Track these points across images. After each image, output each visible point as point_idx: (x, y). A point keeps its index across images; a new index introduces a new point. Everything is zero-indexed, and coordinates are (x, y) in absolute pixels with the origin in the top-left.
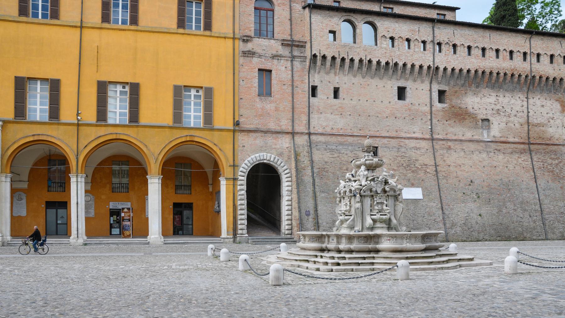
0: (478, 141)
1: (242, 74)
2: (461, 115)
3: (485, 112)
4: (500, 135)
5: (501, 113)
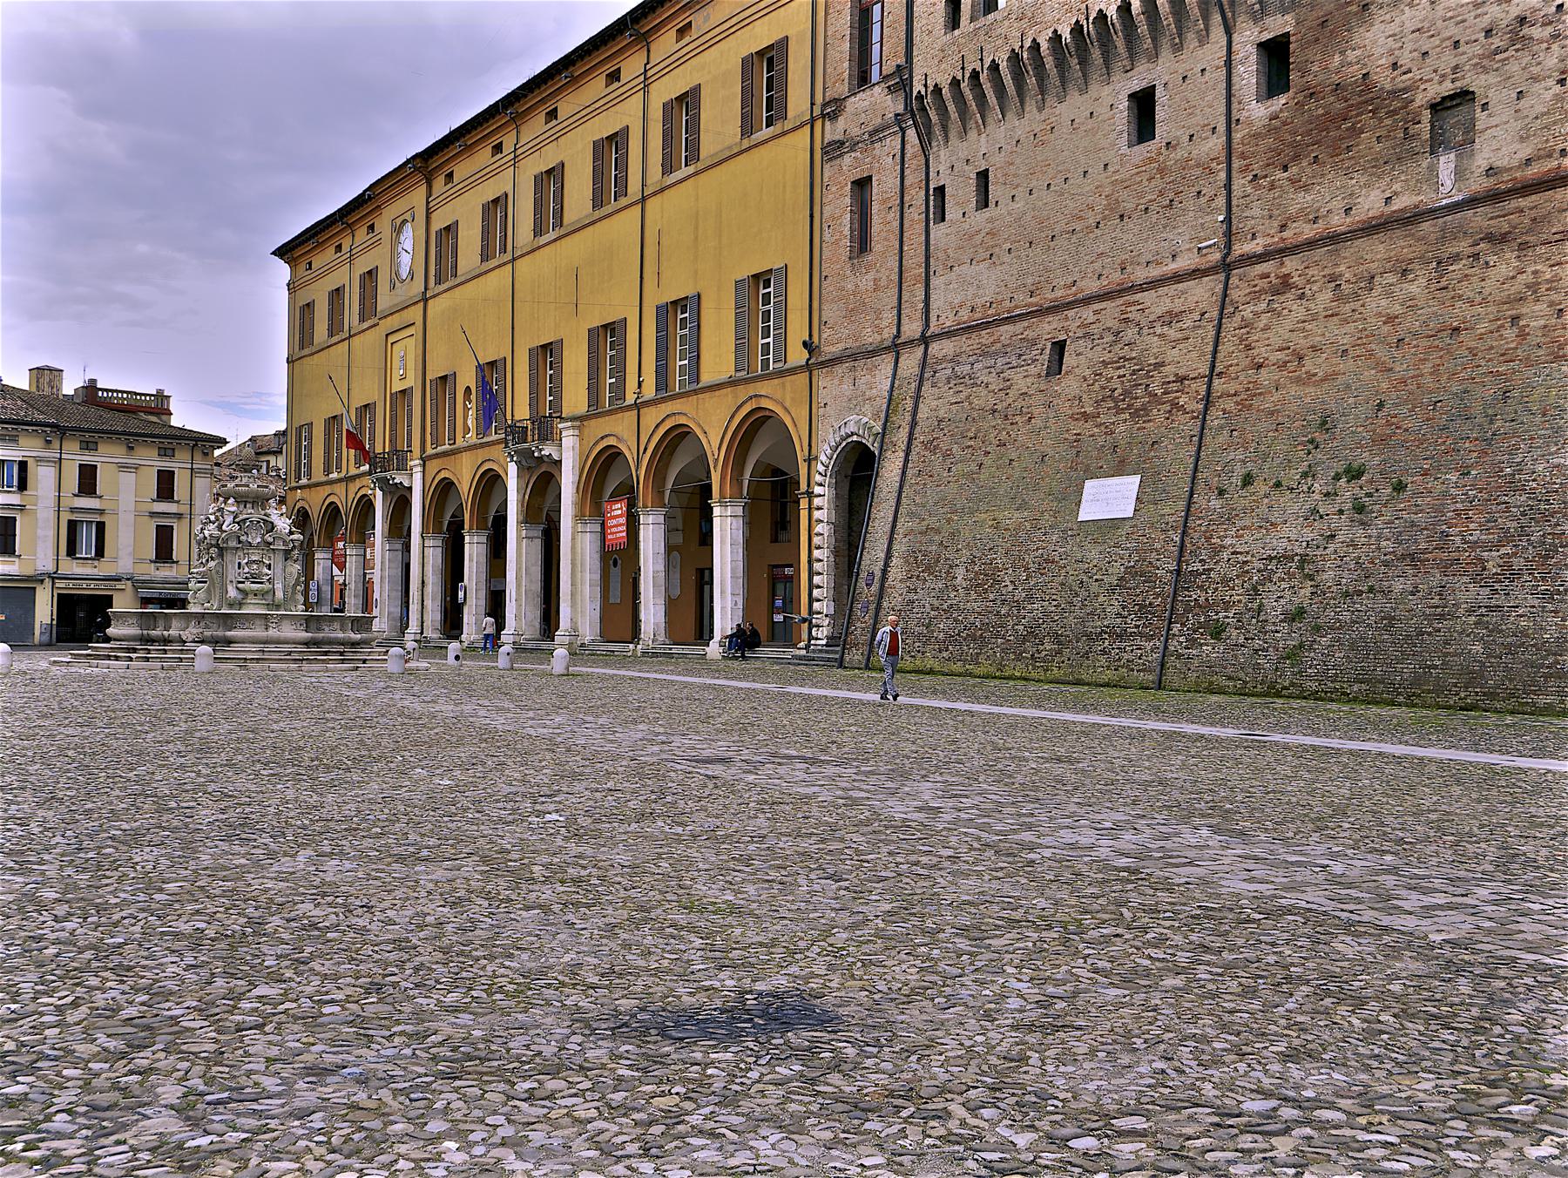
0: (1410, 219)
1: (827, 210)
3: (1448, 60)
4: (1526, 151)
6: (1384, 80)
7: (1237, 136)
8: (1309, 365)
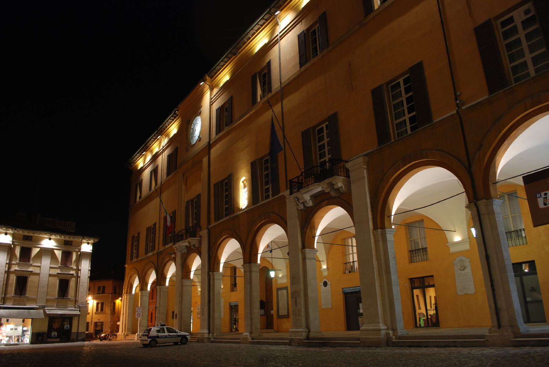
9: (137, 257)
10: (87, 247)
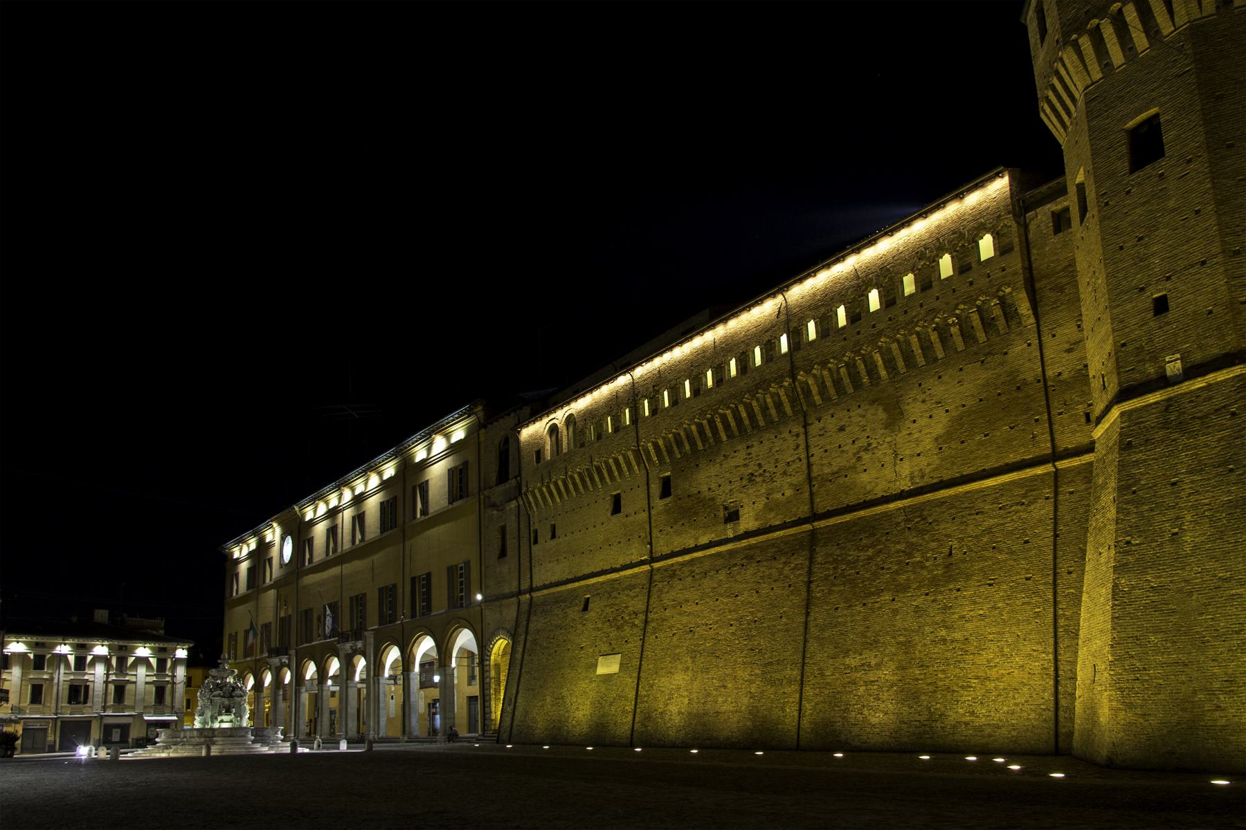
2: (691, 509)
5: (758, 479)
6: (706, 494)
7: (653, 512)
8: (684, 609)
9: (235, 658)
10: (182, 653)
